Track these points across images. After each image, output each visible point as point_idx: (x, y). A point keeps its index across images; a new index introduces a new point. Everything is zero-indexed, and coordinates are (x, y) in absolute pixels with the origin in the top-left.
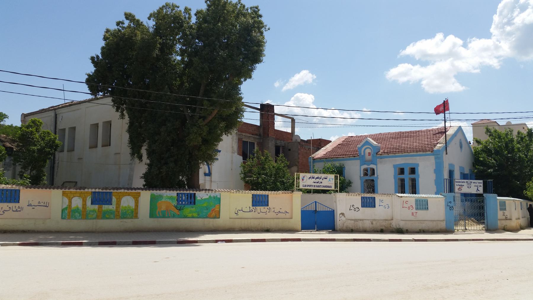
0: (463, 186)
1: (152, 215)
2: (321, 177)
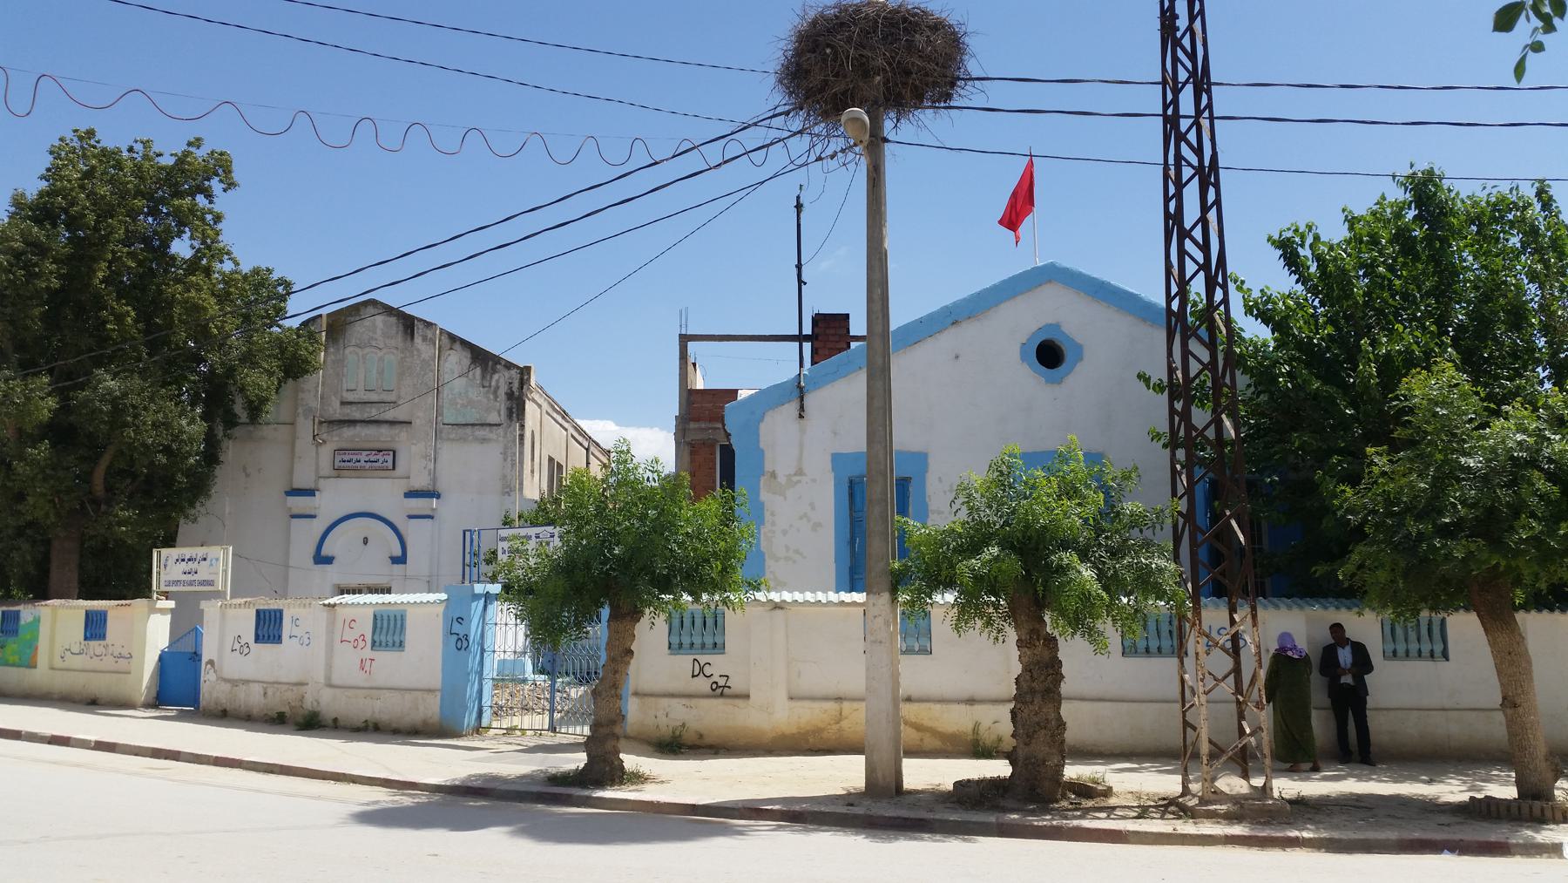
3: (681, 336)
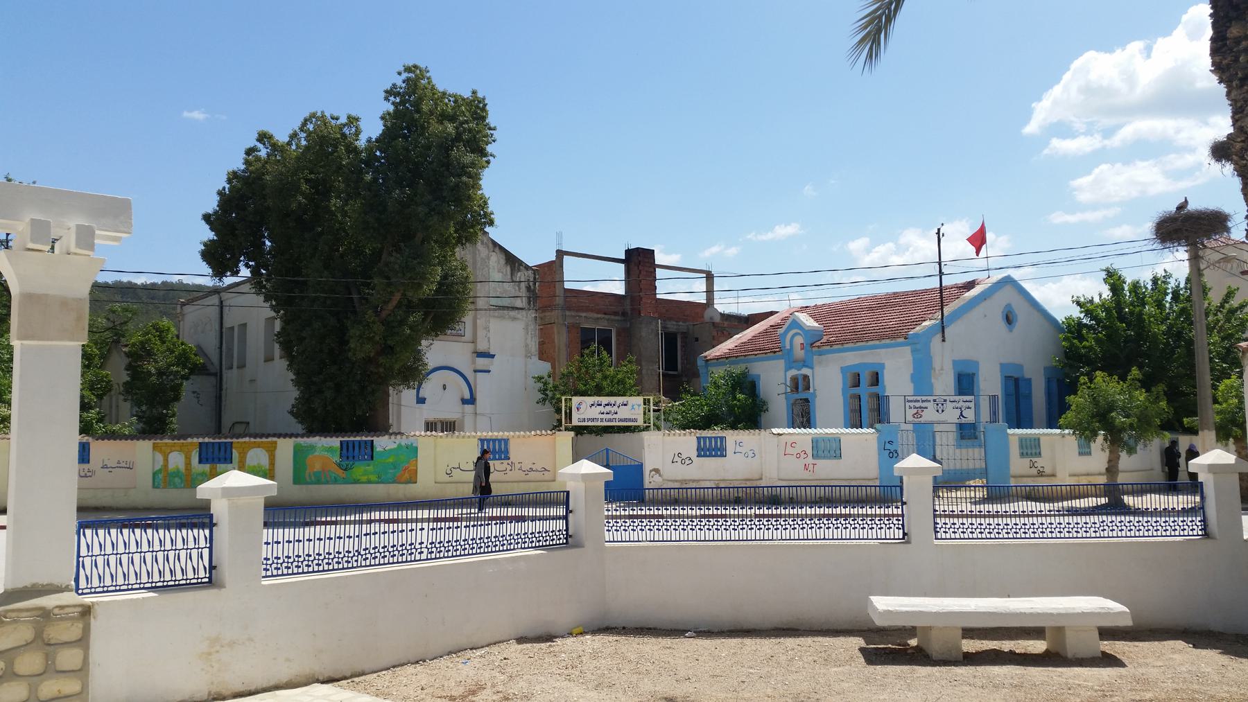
0: (926, 408)
1: (298, 479)
2: (615, 402)
3: (558, 251)
